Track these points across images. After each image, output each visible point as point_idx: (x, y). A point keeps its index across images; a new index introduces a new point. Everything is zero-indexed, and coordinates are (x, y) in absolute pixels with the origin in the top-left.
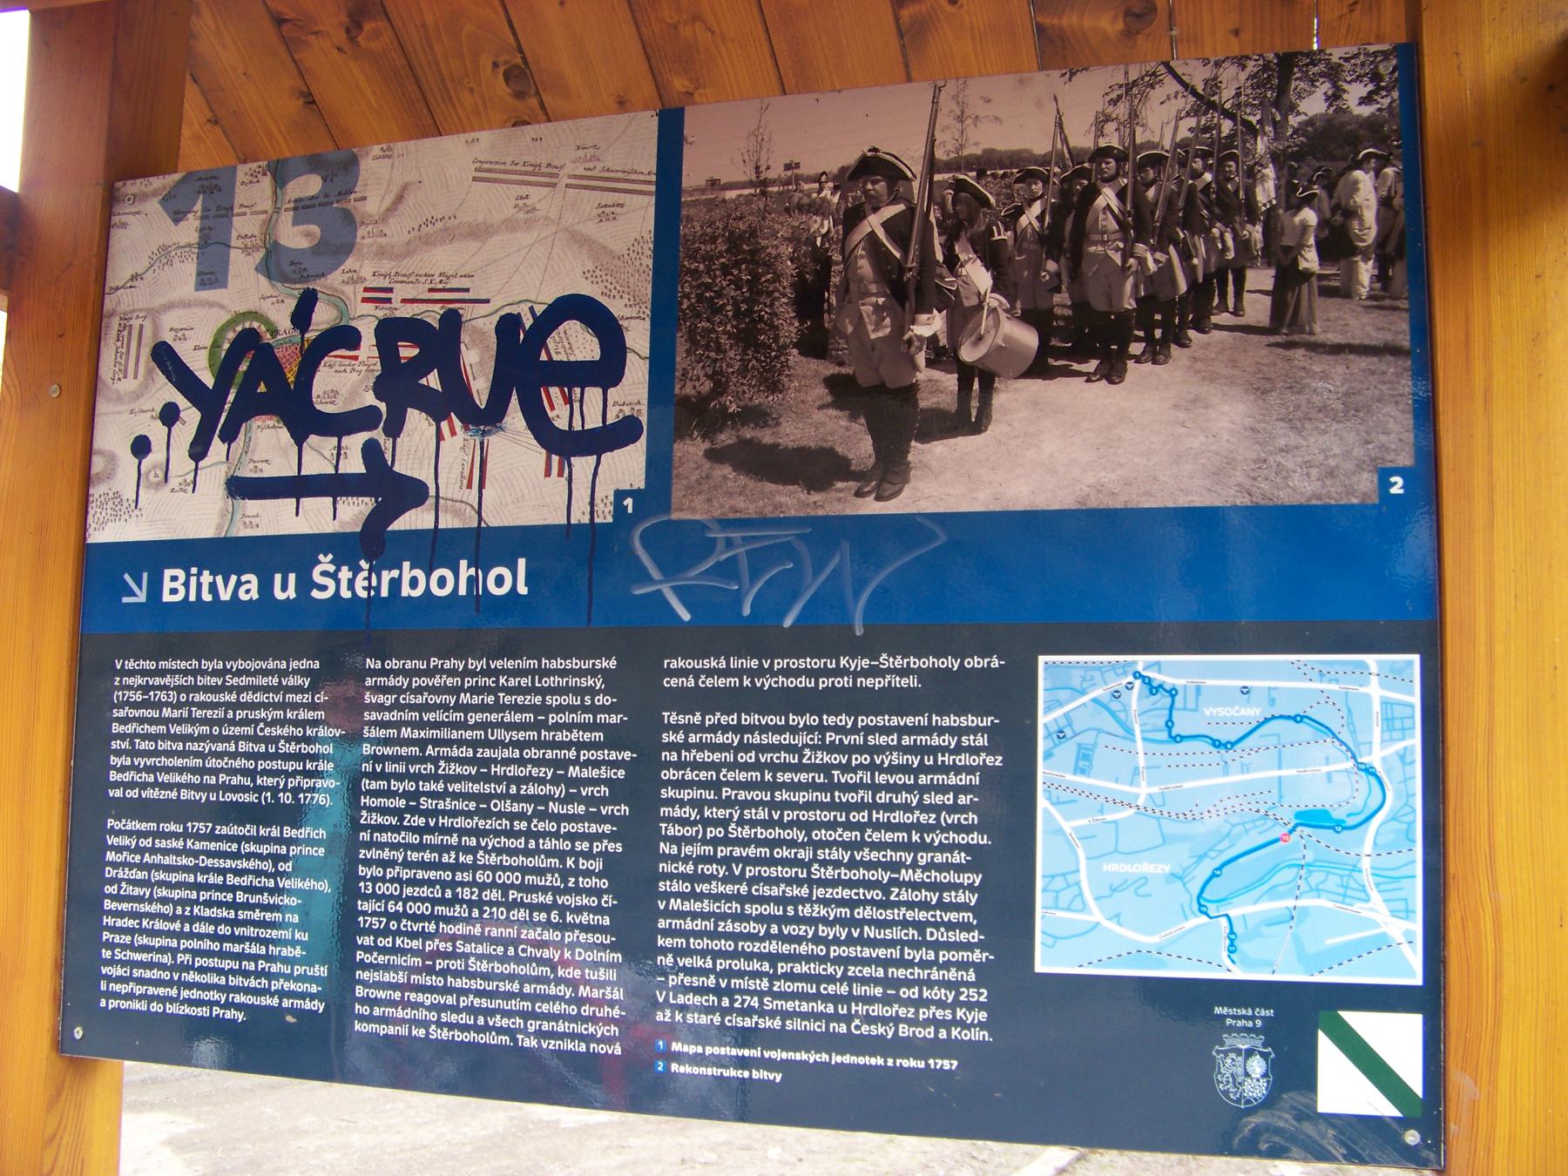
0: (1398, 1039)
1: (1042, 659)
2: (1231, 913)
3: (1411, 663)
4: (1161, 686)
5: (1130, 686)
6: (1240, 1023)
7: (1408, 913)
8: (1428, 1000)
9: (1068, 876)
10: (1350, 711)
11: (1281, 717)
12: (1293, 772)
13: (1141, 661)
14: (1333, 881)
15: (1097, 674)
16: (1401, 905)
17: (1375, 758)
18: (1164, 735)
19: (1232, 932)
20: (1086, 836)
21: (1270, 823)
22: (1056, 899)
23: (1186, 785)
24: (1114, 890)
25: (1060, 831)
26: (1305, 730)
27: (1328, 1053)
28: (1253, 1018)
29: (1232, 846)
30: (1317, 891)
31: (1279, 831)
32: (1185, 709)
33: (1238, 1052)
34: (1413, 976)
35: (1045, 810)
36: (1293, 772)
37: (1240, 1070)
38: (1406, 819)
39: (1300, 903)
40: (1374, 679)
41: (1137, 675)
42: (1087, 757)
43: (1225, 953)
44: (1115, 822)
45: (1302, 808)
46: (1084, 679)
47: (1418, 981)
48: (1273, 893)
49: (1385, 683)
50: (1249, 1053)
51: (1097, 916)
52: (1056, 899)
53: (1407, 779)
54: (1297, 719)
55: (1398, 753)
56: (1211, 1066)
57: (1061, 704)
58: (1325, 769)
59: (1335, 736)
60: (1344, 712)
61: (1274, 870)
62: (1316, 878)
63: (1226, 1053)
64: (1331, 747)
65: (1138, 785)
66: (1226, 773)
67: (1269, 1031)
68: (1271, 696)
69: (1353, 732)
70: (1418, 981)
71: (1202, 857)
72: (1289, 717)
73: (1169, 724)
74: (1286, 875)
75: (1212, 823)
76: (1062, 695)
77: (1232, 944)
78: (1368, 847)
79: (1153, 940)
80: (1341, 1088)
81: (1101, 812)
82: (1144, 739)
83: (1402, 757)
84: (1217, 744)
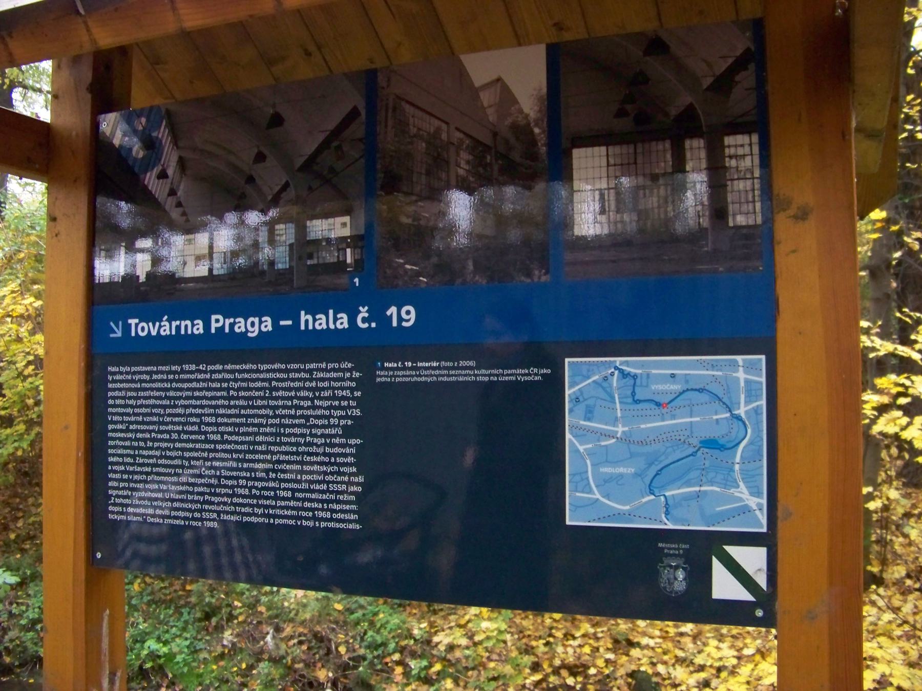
0: (754, 559)
1: (567, 360)
2: (667, 494)
3: (760, 360)
4: (629, 374)
5: (612, 374)
6: (672, 552)
7: (758, 494)
9: (581, 474)
10: (728, 386)
11: (692, 390)
12: (698, 419)
13: (618, 360)
14: (719, 477)
15: (595, 368)
16: (755, 490)
17: (742, 411)
18: (630, 400)
19: (667, 504)
20: (590, 453)
21: (686, 446)
22: (576, 487)
23: (643, 426)
24: (605, 481)
25: (578, 451)
26: (704, 397)
27: (718, 567)
28: (678, 549)
29: (667, 458)
30: (711, 483)
32: (641, 386)
33: (671, 566)
34: (762, 527)
35: (570, 440)
36: (698, 419)
37: (672, 577)
38: (759, 444)
39: (703, 489)
40: (741, 369)
41: (616, 368)
42: (591, 412)
43: (663, 515)
44: (606, 446)
45: (703, 438)
46: (588, 371)
47: (764, 530)
48: (688, 484)
50: (676, 568)
51: (598, 496)
52: (576, 487)
54: (700, 390)
55: (751, 407)
56: (657, 574)
57: (578, 384)
58: (715, 417)
59: (720, 400)
60: (725, 385)
61: (689, 470)
62: (711, 475)
63: (664, 567)
64: (717, 405)
65: (617, 427)
66: (663, 420)
68: (687, 379)
69: (730, 398)
70: (764, 530)
71: (650, 465)
72: (696, 390)
73: (633, 394)
74: (694, 474)
76: (577, 379)
77: (667, 510)
78: (738, 459)
79: (628, 507)
80: (724, 587)
81: (599, 441)
82: (620, 402)
83: (757, 411)
84: (658, 404)
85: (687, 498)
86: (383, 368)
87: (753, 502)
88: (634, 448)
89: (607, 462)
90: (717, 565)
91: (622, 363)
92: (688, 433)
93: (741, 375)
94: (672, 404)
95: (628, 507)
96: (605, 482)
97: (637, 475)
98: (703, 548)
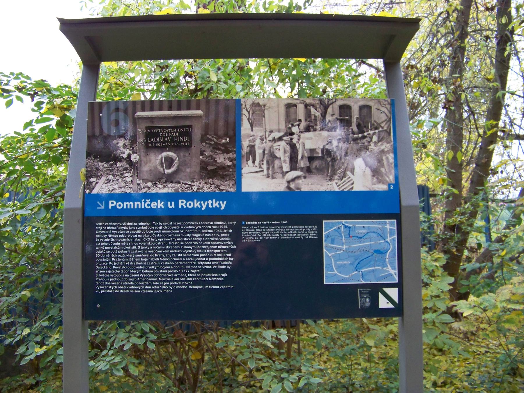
0: (393, 293)
1: (324, 221)
4: (347, 226)
5: (341, 227)
7: (395, 269)
8: (399, 285)
13: (343, 221)
17: (388, 240)
20: (333, 256)
25: (328, 256)
26: (375, 235)
27: (381, 296)
30: (378, 266)
31: (371, 254)
41: (343, 224)
42: (333, 241)
48: (370, 267)
49: (390, 225)
50: (366, 298)
51: (336, 273)
53: (394, 244)
55: (392, 239)
61: (370, 262)
62: (378, 263)
66: (360, 243)
67: (370, 293)
70: (397, 282)
71: (356, 260)
73: (349, 234)
74: (372, 263)
75: (358, 253)
76: (328, 228)
78: (387, 257)
79: (347, 276)
80: (383, 303)
83: (394, 239)
84: (359, 238)
85: (370, 272)
86: (246, 225)
87: (393, 272)
88: (350, 254)
89: (340, 260)
90: (380, 295)
91: (345, 222)
92: (369, 248)
93: (388, 227)
94: (364, 237)
95: (347, 276)
96: (339, 267)
97: (351, 264)
98: (375, 290)
